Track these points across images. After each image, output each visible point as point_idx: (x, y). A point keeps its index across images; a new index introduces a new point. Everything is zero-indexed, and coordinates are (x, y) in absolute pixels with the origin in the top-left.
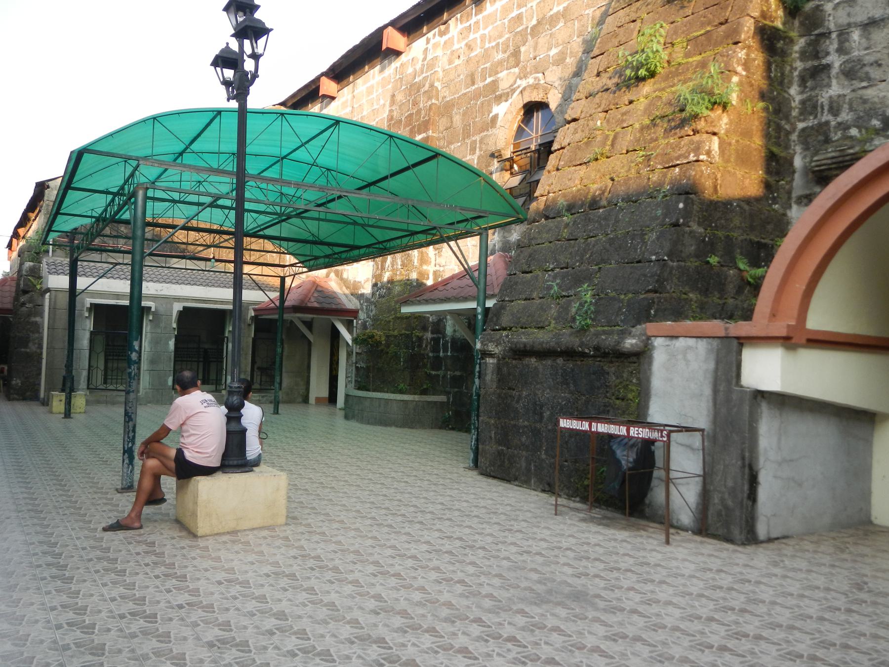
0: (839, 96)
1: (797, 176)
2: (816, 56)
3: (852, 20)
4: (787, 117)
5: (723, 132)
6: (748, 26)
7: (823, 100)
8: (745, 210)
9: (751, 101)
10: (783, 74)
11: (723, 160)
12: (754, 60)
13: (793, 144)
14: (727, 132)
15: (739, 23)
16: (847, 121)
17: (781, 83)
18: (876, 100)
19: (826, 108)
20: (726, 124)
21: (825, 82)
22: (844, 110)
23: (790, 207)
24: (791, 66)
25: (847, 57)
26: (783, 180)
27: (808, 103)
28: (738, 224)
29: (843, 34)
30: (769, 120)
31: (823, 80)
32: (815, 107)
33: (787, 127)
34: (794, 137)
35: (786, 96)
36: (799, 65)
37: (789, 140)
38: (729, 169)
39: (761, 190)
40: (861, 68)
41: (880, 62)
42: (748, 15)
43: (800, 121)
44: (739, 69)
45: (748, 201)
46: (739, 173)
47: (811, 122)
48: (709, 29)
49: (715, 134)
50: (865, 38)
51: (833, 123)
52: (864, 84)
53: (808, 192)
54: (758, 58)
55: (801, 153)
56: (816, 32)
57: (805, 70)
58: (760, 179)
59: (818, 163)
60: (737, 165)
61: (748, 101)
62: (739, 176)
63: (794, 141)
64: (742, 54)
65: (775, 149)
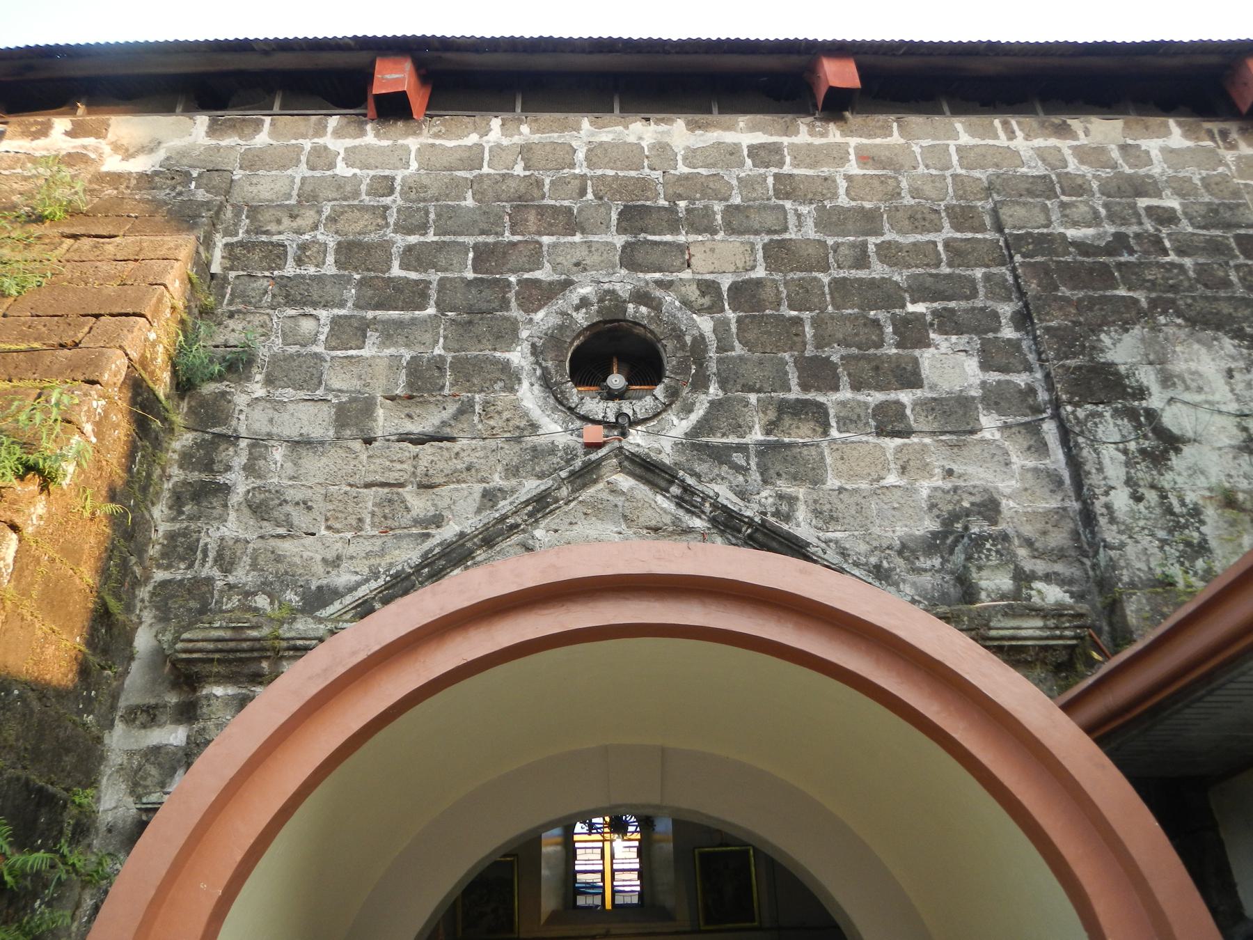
0: (237, 541)
1: (134, 666)
2: (208, 466)
3: (275, 430)
4: (140, 552)
5: (30, 529)
6: (115, 369)
7: (208, 540)
8: (32, 712)
9: (93, 495)
10: (149, 476)
11: (16, 587)
12: (116, 426)
13: (139, 605)
14: (39, 533)
15: (102, 354)
16: (245, 585)
17: (144, 489)
18: (297, 560)
19: (212, 555)
20: (41, 517)
21: (216, 513)
22: (242, 564)
23: (111, 726)
24: (164, 471)
25: (259, 482)
26: (110, 668)
27: (182, 539)
28: (11, 740)
29: (259, 444)
30: (112, 543)
31: (214, 508)
32: (192, 549)
33: (138, 570)
34: (144, 593)
35: (148, 516)
36: (177, 473)
37: (134, 596)
38: (24, 611)
39: (70, 676)
40: (281, 505)
41: (310, 504)
42: (121, 347)
43: (159, 566)
44: (88, 428)
45: (41, 690)
46: (40, 629)
47: (180, 573)
48: (36, 345)
49: (14, 528)
50: (292, 461)
51: (219, 584)
52: (281, 531)
53: (153, 701)
54: (121, 429)
55: (151, 625)
56: (216, 430)
57: (185, 483)
58: (73, 653)
59: (190, 645)
60: (39, 608)
61: (89, 491)
62: (39, 633)
63: (142, 601)
64: (98, 405)
65: (112, 603)
